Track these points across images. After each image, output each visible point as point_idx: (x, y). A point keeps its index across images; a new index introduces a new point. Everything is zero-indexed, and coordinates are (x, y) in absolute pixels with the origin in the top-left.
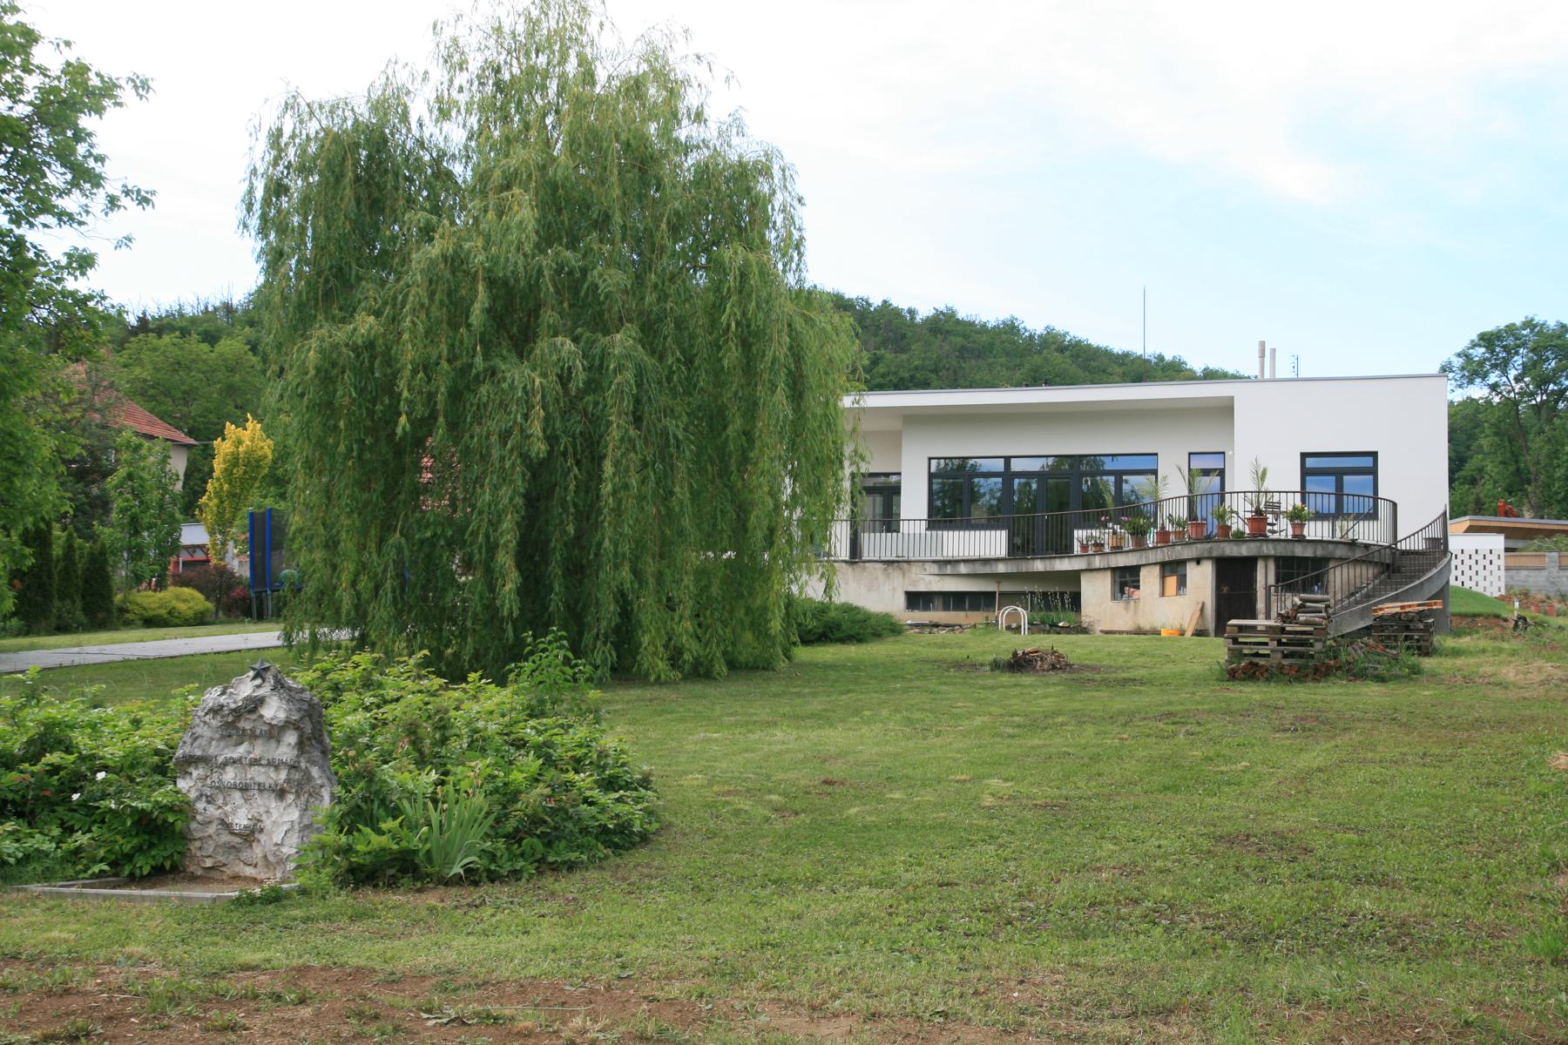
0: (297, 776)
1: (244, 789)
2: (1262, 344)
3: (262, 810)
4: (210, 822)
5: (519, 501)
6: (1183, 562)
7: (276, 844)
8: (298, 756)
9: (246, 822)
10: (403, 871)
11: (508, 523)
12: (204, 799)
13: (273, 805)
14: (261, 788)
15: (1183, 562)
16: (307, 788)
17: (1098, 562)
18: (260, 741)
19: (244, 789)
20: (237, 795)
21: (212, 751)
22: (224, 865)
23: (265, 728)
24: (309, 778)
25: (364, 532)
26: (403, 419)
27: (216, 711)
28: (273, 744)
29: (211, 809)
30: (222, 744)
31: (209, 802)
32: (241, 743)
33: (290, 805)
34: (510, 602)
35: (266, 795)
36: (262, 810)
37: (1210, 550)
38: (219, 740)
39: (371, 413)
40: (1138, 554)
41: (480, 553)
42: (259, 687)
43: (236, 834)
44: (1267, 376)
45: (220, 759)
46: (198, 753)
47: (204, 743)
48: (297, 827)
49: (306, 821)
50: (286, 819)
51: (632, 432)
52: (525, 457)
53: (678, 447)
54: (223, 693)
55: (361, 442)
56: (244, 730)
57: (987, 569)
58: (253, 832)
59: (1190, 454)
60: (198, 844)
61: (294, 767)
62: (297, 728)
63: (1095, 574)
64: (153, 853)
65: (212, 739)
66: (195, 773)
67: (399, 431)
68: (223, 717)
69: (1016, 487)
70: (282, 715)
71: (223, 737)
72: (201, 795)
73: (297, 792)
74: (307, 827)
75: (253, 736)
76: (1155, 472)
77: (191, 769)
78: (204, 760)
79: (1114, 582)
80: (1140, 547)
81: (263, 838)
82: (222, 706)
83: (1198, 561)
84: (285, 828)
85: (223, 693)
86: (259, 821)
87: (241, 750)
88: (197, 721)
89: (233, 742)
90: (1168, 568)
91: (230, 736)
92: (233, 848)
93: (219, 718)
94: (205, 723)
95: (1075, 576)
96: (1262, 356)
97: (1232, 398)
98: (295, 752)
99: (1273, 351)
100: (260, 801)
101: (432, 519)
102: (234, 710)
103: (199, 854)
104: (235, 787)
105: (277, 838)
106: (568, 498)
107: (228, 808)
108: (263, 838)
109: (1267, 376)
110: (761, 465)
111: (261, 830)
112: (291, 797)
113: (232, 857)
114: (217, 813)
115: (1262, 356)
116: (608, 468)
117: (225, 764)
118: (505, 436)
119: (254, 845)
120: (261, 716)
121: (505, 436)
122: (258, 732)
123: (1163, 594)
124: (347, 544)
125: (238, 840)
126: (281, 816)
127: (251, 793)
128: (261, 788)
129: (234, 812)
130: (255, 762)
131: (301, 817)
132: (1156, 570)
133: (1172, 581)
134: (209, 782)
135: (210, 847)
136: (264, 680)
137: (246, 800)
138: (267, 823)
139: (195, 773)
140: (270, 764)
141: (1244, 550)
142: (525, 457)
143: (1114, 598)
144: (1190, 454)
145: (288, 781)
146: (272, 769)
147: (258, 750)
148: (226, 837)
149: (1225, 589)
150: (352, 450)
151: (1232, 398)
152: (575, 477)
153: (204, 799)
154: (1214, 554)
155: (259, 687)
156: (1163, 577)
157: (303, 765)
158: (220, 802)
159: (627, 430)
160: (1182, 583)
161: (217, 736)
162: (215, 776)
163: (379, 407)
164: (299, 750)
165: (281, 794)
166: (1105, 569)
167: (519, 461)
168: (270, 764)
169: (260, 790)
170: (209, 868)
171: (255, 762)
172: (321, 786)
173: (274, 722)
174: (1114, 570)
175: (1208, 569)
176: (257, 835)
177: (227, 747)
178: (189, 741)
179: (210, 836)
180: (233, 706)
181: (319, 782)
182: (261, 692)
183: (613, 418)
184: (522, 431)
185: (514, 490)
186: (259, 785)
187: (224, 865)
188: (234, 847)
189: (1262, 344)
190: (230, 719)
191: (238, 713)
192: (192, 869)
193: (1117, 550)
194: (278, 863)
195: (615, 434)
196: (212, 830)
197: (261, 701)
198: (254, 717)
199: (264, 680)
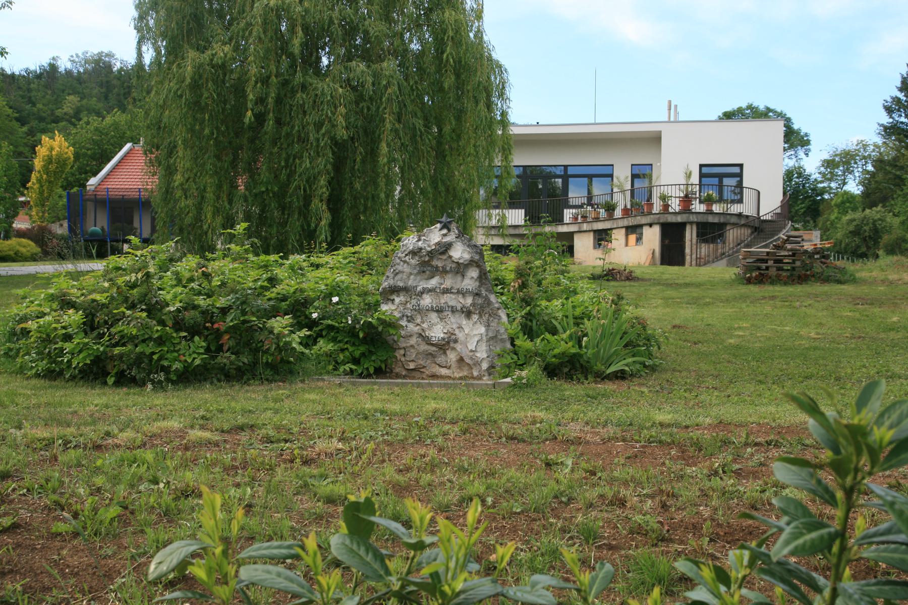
0: (480, 301)
1: (439, 311)
2: (670, 102)
3: (454, 326)
4: (411, 336)
5: (329, 167)
6: (641, 226)
7: (472, 351)
8: (479, 287)
9: (442, 335)
10: (574, 368)
11: (323, 181)
12: (405, 319)
13: (464, 322)
14: (453, 310)
15: (641, 226)
16: (487, 310)
17: (585, 227)
18: (450, 275)
19: (439, 311)
20: (434, 316)
21: (411, 283)
22: (424, 367)
23: (454, 265)
24: (489, 303)
25: (219, 187)
26: (249, 113)
27: (414, 253)
28: (459, 278)
29: (411, 326)
30: (418, 278)
31: (409, 321)
32: (433, 277)
33: (476, 323)
34: (325, 232)
35: (457, 315)
36: (454, 326)
37: (659, 218)
38: (416, 275)
39: (224, 109)
40: (611, 222)
41: (298, 201)
42: (445, 235)
43: (432, 345)
44: (672, 119)
45: (419, 289)
46: (401, 284)
47: (405, 277)
48: (484, 338)
49: (491, 334)
50: (475, 332)
51: (397, 125)
52: (333, 139)
53: (421, 137)
54: (419, 240)
55: (217, 128)
56: (437, 267)
57: (517, 232)
58: (448, 343)
59: (632, 165)
60: (402, 352)
61: (477, 295)
62: (478, 266)
63: (582, 234)
64: (373, 358)
65: (411, 274)
66: (397, 300)
67: (247, 120)
68: (421, 257)
69: (556, 180)
70: (467, 256)
71: (419, 273)
72: (403, 316)
73: (479, 313)
74: (492, 338)
75: (444, 272)
76: (611, 176)
77: (394, 297)
78: (406, 290)
79: (595, 238)
80: (610, 217)
81: (458, 347)
82: (421, 249)
83: (651, 225)
84: (476, 339)
85: (419, 240)
86: (452, 334)
87: (434, 282)
88: (398, 261)
89: (426, 277)
90: (630, 230)
91: (424, 272)
92: (432, 355)
93: (417, 258)
94: (405, 262)
95: (570, 236)
96: (670, 109)
97: (661, 132)
98: (477, 284)
99: (676, 106)
100: (453, 320)
101: (265, 180)
102: (430, 252)
103: (403, 359)
104: (432, 309)
105: (472, 347)
106: (356, 167)
107: (425, 325)
108: (458, 347)
109: (672, 119)
110: (468, 150)
111: (456, 341)
112: (475, 317)
113: (429, 361)
114: (416, 329)
115: (670, 109)
116: (384, 148)
117: (422, 293)
118: (319, 126)
119: (448, 352)
120: (450, 257)
121: (319, 126)
122: (448, 269)
123: (627, 245)
124: (210, 195)
125: (434, 349)
126: (472, 330)
127: (445, 313)
128: (453, 310)
129: (431, 326)
130: (446, 291)
131: (487, 331)
132: (623, 231)
133: (632, 238)
134: (408, 305)
135: (412, 354)
136: (449, 230)
137: (441, 319)
138: (460, 335)
139: (397, 300)
140: (459, 292)
141: (679, 219)
142: (333, 139)
143: (595, 248)
144: (632, 165)
145: (473, 305)
146: (461, 296)
147: (448, 282)
148: (424, 347)
149: (667, 242)
150: (213, 134)
151: (661, 132)
152: (361, 153)
153: (405, 319)
154: (661, 221)
155: (445, 235)
156: (627, 235)
157: (484, 293)
158: (419, 321)
159: (394, 124)
160: (639, 240)
161: (415, 271)
162: (414, 302)
163: (228, 106)
164: (480, 282)
165: (468, 314)
166: (589, 231)
167: (329, 141)
168: (459, 292)
169: (453, 312)
170: (412, 370)
171: (446, 291)
172: (498, 309)
173: (461, 261)
174: (595, 231)
175: (657, 229)
176: (452, 345)
177: (421, 280)
178: (392, 276)
179: (412, 346)
180: (429, 249)
181: (497, 305)
182: (447, 239)
183: (387, 116)
184: (330, 121)
185: (327, 160)
186: (452, 307)
187: (424, 367)
188: (431, 354)
189: (670, 102)
190: (427, 259)
191: (431, 254)
192: (397, 370)
193: (597, 219)
194: (474, 364)
195: (388, 126)
196: (413, 341)
197: (449, 246)
198: (444, 257)
199: (449, 230)
